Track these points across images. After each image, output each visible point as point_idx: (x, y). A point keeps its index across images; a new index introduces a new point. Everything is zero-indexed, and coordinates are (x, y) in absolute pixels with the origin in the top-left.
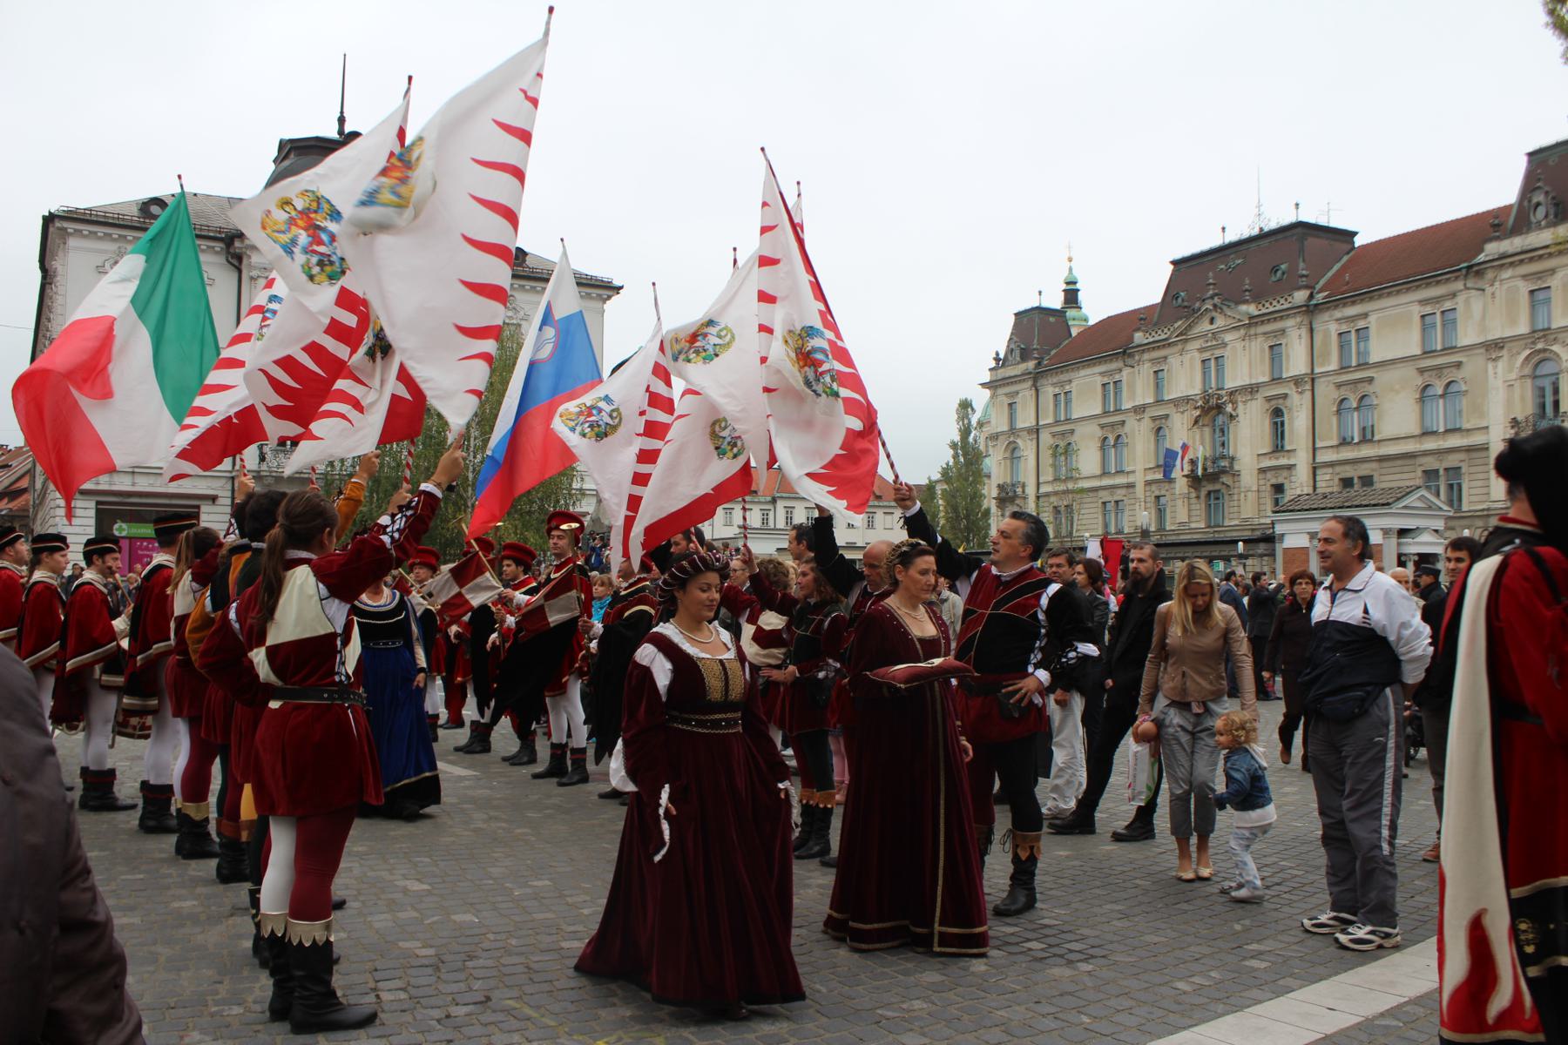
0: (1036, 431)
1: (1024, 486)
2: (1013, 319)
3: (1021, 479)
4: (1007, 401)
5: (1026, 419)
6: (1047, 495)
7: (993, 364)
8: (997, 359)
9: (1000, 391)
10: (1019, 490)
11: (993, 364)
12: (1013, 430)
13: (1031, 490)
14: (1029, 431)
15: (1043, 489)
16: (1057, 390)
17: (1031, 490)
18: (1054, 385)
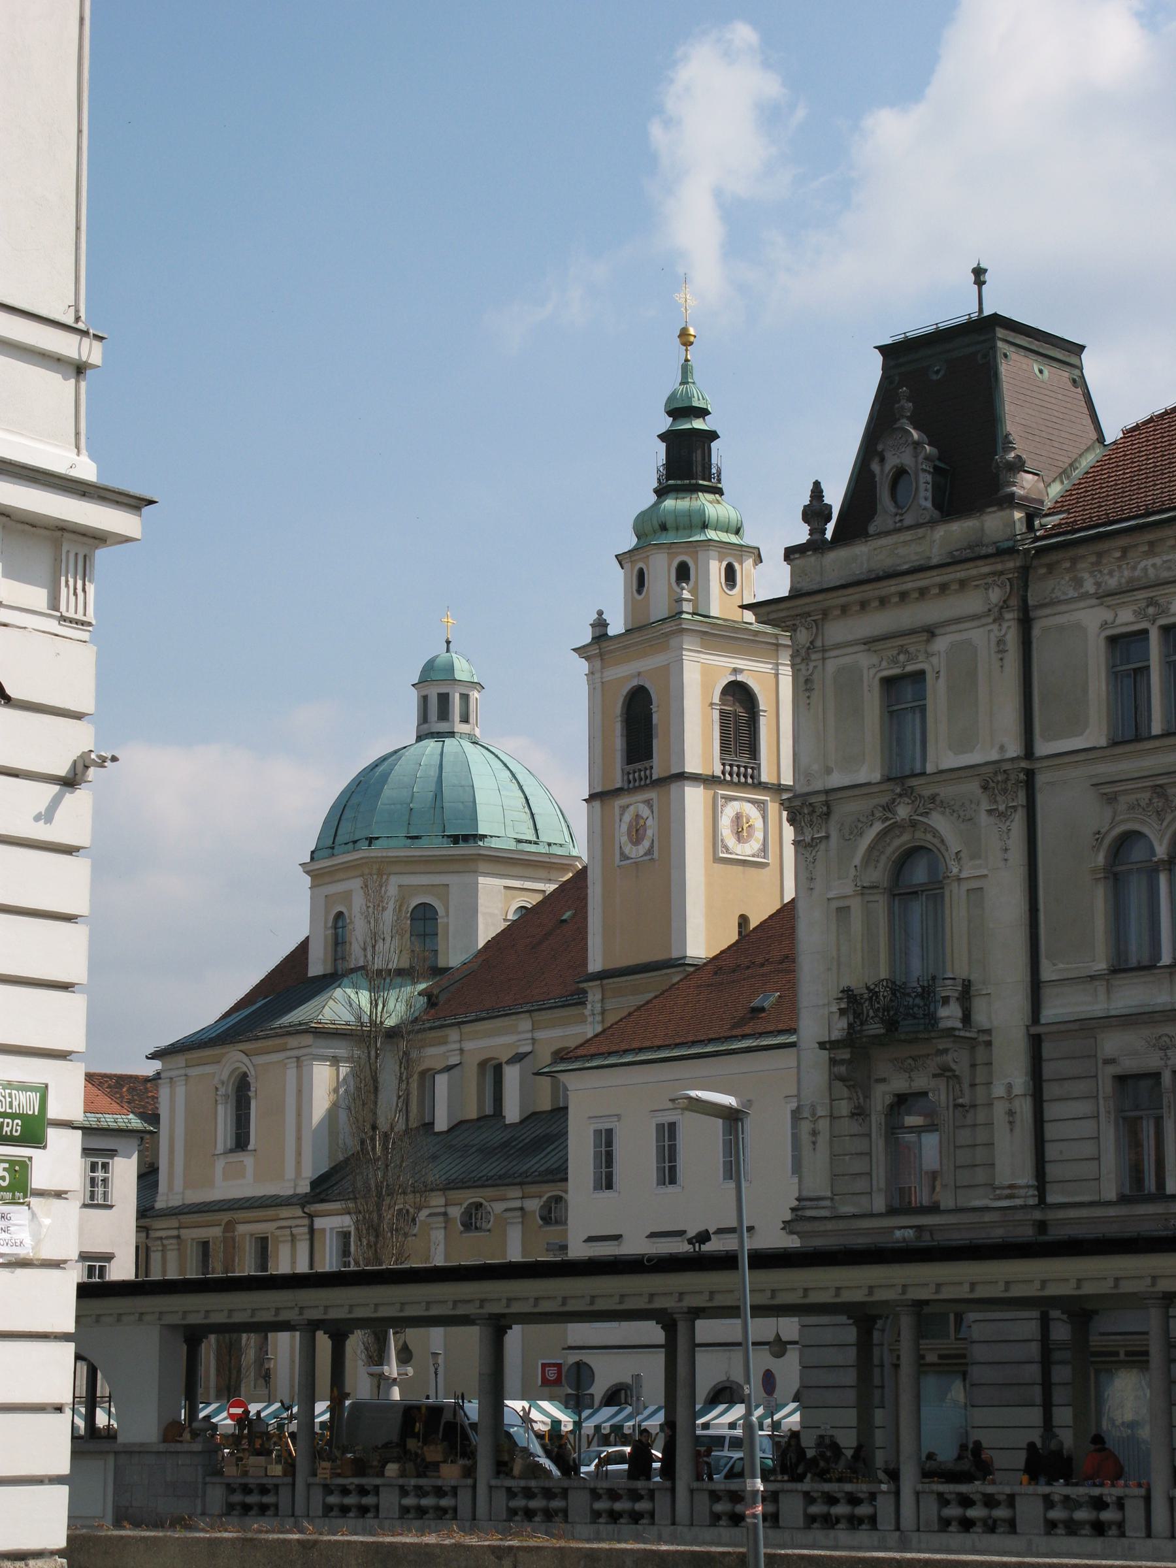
0: (1019, 783)
1: (966, 994)
2: (878, 359)
3: (959, 966)
4: (871, 669)
5: (973, 730)
6: (1088, 1027)
7: (801, 534)
8: (815, 512)
9: (837, 631)
10: (950, 1014)
11: (801, 534)
12: (902, 779)
13: (1003, 1012)
14: (992, 778)
15: (1055, 1009)
16: (1126, 618)
17: (1003, 1012)
18: (1104, 596)
